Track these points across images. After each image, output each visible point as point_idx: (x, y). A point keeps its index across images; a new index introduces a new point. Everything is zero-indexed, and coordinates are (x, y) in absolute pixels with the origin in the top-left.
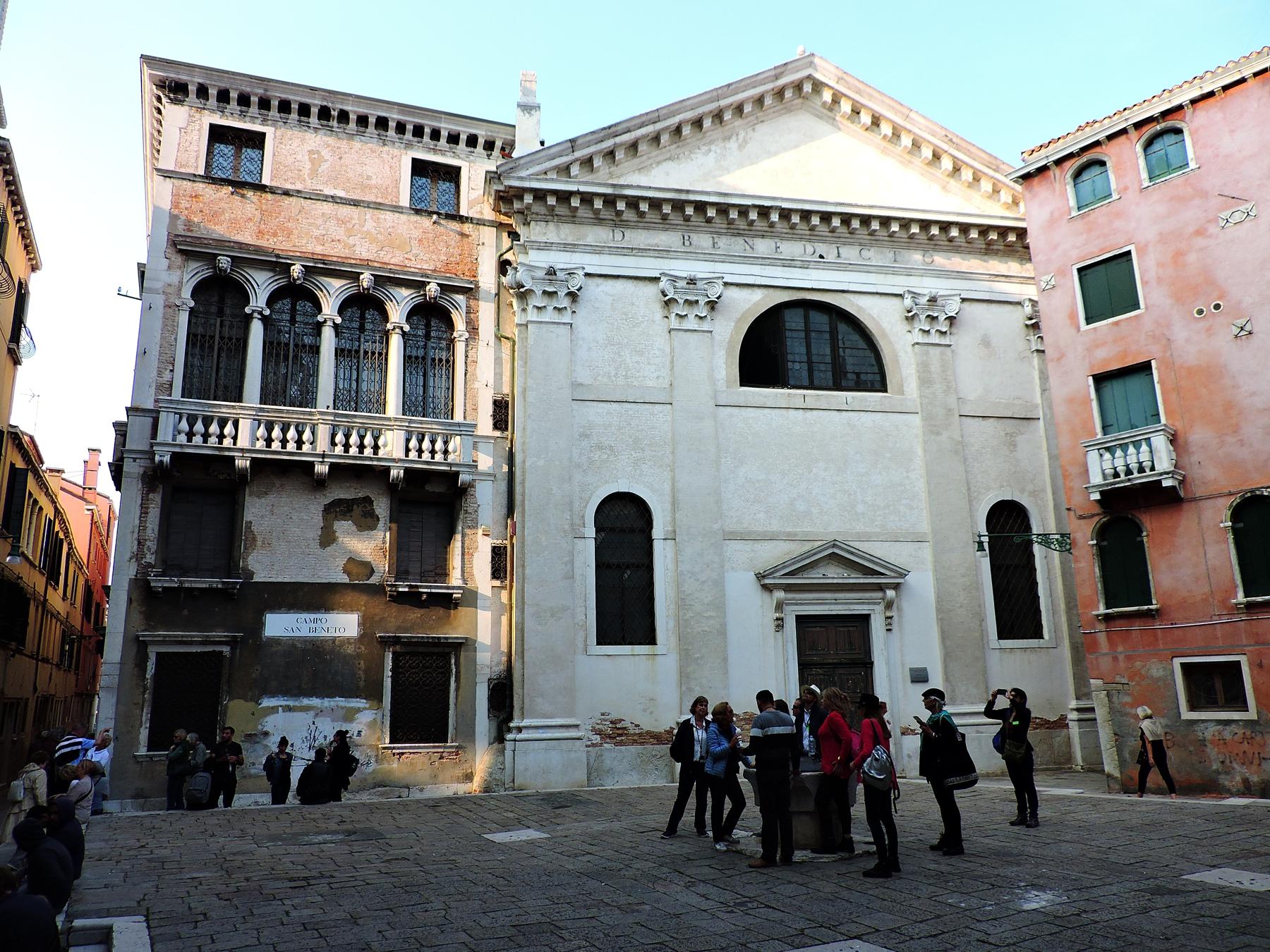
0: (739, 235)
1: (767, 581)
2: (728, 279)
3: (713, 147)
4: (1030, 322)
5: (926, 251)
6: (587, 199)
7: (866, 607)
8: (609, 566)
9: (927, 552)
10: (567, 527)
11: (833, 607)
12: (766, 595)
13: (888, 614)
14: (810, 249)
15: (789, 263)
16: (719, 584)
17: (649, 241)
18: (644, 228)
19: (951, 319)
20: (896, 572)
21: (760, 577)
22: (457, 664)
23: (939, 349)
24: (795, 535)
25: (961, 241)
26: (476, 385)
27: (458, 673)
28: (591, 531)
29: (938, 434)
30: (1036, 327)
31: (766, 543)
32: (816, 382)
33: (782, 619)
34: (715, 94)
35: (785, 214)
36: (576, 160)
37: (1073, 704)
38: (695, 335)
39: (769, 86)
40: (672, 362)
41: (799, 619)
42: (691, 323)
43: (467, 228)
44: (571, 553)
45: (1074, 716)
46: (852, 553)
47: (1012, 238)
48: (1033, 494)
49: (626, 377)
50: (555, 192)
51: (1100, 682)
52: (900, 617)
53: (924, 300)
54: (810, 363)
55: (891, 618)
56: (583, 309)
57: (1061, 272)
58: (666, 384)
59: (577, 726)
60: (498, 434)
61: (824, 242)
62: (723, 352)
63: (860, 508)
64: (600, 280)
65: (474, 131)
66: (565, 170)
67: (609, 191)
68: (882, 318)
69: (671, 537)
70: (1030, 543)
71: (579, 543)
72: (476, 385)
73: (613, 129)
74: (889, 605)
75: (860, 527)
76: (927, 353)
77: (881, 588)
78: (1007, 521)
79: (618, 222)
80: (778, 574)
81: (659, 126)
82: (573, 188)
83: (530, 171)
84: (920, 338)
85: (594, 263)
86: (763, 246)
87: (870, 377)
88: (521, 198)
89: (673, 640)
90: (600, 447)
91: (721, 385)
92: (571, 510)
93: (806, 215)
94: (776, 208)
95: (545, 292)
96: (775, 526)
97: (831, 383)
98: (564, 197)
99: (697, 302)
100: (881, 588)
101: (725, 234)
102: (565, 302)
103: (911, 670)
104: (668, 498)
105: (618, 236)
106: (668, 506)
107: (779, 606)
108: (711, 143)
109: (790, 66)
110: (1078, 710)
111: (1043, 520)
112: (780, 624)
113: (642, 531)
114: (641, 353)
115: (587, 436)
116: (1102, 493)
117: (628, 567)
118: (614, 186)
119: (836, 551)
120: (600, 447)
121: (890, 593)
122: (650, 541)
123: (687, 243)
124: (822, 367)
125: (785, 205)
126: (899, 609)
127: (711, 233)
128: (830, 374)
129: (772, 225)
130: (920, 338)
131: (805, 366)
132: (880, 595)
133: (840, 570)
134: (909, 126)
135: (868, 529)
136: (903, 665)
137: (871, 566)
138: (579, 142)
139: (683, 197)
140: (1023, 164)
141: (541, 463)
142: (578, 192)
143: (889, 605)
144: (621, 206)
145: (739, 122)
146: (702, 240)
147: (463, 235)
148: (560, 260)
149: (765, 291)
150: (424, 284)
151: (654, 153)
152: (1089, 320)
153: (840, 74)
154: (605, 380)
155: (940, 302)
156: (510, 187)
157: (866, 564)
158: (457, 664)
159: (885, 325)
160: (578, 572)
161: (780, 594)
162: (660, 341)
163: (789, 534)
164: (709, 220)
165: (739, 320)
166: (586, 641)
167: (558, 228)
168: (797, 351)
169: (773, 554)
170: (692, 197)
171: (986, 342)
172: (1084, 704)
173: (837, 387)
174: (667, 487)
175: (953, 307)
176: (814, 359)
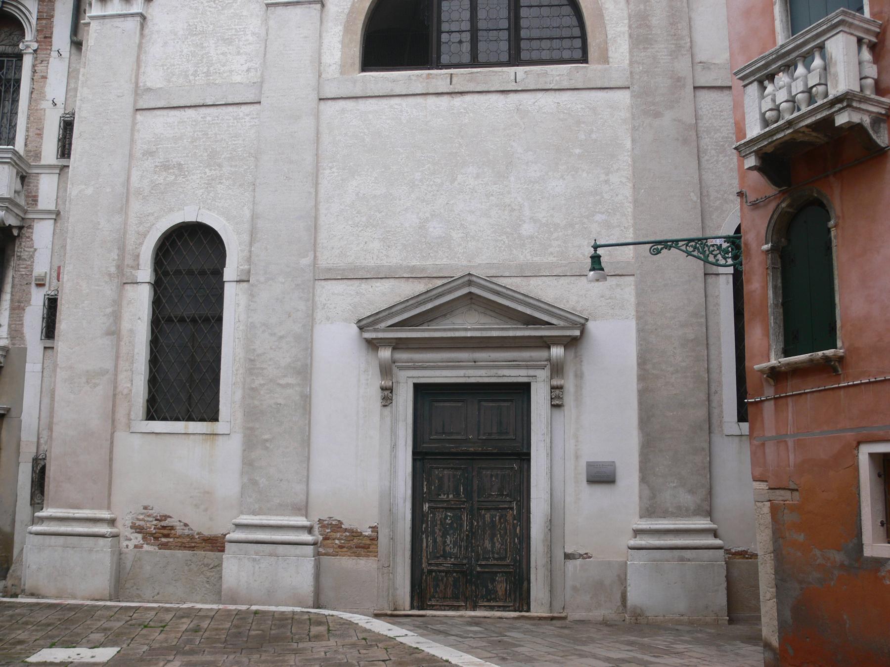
7: (523, 372)
16: (305, 342)
24: (423, 269)
29: (657, 115)
32: (482, 58)
33: (391, 390)
41: (420, 390)
46: (498, 293)
49: (208, 74)
52: (579, 388)
54: (474, 31)
63: (527, 229)
75: (524, 256)
77: (545, 343)
80: (383, 325)
90: (165, 167)
96: (395, 258)
106: (246, 237)
107: (386, 370)
112: (387, 395)
114: (229, 41)
119: (474, 290)
120: (165, 167)
126: (579, 376)
131: (466, 37)
133: (484, 319)
137: (528, 311)
141: (90, 191)
154: (181, 81)
157: (520, 308)
162: (254, 24)
163: (413, 269)
168: (455, 16)
169: (382, 295)
176: (481, 25)
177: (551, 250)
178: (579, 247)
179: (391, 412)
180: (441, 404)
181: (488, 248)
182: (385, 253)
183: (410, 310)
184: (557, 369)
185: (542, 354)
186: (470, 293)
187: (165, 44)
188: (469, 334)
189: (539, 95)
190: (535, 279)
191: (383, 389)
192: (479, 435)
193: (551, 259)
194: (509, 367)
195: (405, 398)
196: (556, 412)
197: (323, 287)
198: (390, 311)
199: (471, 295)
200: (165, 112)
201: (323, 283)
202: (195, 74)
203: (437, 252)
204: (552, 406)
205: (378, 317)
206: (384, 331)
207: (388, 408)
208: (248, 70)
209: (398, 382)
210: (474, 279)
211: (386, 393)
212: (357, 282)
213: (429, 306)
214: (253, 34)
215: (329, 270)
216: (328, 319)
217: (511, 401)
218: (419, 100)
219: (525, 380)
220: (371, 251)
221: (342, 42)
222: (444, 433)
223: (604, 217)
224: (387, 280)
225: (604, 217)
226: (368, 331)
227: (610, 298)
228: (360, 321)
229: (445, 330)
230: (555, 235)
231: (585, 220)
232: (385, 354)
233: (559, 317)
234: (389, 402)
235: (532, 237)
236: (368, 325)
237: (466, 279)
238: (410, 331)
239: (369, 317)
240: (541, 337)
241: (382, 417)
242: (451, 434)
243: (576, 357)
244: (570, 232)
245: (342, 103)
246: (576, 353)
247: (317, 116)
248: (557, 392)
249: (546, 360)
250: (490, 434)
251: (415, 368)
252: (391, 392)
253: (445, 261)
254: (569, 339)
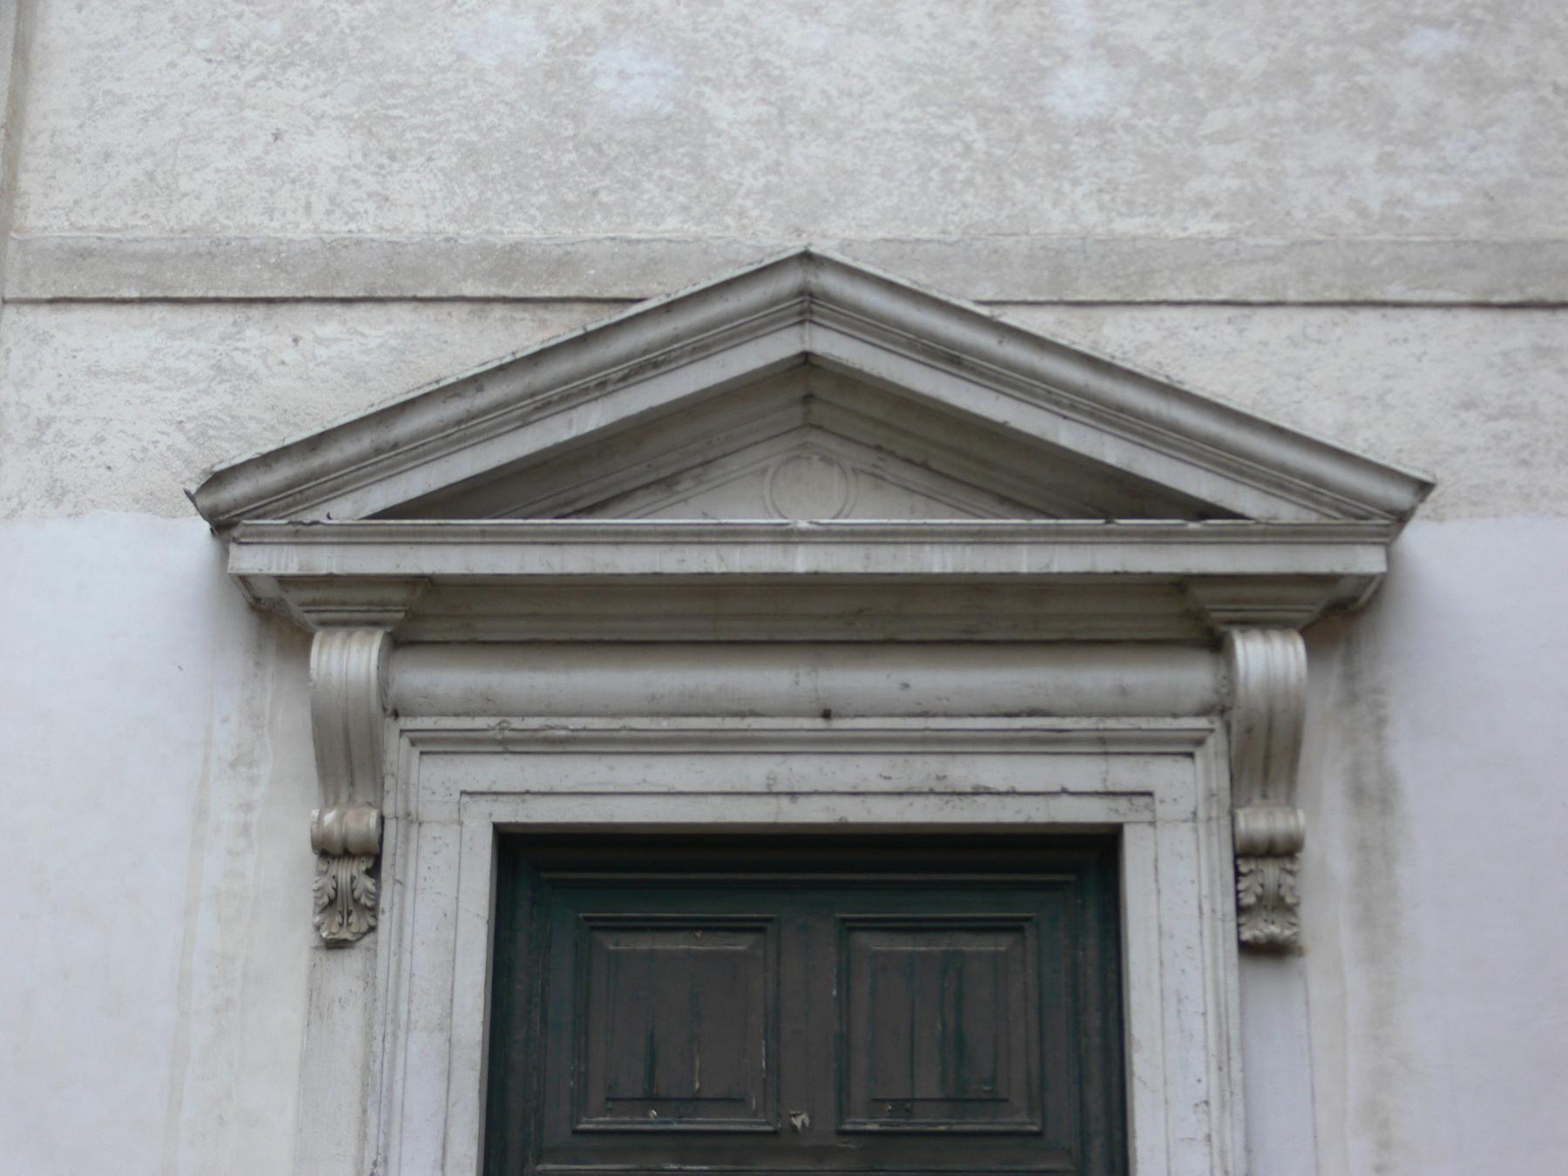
7: (1082, 772)
24: (566, 263)
33: (372, 856)
46: (951, 358)
52: (1375, 857)
55: (1285, 851)
63: (1079, 89)
75: (1071, 210)
77: (1196, 618)
80: (343, 510)
96: (419, 209)
100: (1196, 618)
107: (348, 751)
112: (351, 886)
121: (1267, 658)
126: (1374, 796)
133: (873, 510)
137: (1112, 451)
161: (348, 659)
163: (511, 257)
177: (1198, 185)
178: (1340, 173)
179: (369, 981)
180: (643, 943)
181: (886, 173)
182: (371, 183)
183: (490, 435)
184: (1264, 752)
185: (1191, 677)
186: (806, 360)
188: (802, 561)
190: (1125, 315)
192: (842, 1111)
193: (1199, 226)
194: (1007, 744)
195: (445, 907)
196: (1265, 974)
197: (43, 339)
198: (382, 436)
199: (816, 371)
201: (44, 318)
203: (635, 186)
204: (1249, 949)
205: (316, 462)
206: (348, 535)
207: (352, 961)
209: (411, 819)
210: (830, 282)
211: (345, 872)
212: (221, 319)
213: (592, 418)
215: (80, 255)
216: (56, 493)
217: (1013, 927)
219: (1093, 813)
220: (308, 178)
222: (652, 1099)
223: (1452, 41)
224: (377, 311)
225: (1452, 41)
226: (260, 539)
227: (1507, 412)
228: (217, 479)
229: (672, 537)
230: (1217, 120)
231: (1361, 56)
232: (348, 659)
233: (1276, 480)
234: (358, 923)
235: (1101, 126)
236: (260, 506)
237: (789, 281)
238: (486, 538)
239: (266, 460)
240: (1181, 584)
241: (317, 1005)
242: (696, 1101)
243: (1352, 698)
244: (1288, 106)
246: (1350, 677)
248: (1271, 872)
249: (1204, 712)
250: (904, 1106)
251: (506, 745)
252: (374, 872)
253: (672, 225)
254: (1321, 597)
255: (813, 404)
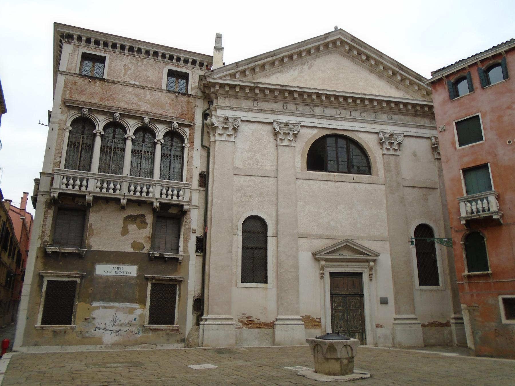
0: (308, 105)
1: (317, 257)
2: (303, 124)
3: (297, 68)
4: (433, 146)
5: (389, 114)
6: (242, 88)
7: (361, 269)
8: (248, 248)
9: (387, 246)
10: (230, 230)
11: (346, 269)
12: (317, 263)
13: (371, 273)
14: (338, 112)
15: (329, 118)
16: (296, 257)
17: (268, 107)
18: (267, 101)
19: (399, 144)
20: (374, 254)
21: (314, 254)
22: (180, 290)
23: (393, 157)
24: (330, 236)
25: (404, 110)
26: (192, 167)
27: (180, 294)
28: (240, 232)
29: (394, 194)
30: (437, 148)
31: (317, 240)
32: (340, 170)
34: (298, 45)
35: (328, 96)
36: (238, 72)
37: (453, 316)
38: (288, 148)
39: (322, 42)
40: (277, 159)
41: (332, 274)
42: (286, 143)
43: (191, 99)
44: (231, 242)
45: (453, 321)
46: (355, 245)
47: (426, 109)
48: (435, 221)
49: (257, 165)
50: (229, 85)
51: (465, 305)
53: (387, 135)
55: (372, 274)
56: (240, 135)
57: (449, 124)
58: (274, 168)
59: (231, 319)
60: (201, 188)
61: (345, 109)
62: (300, 156)
63: (359, 225)
64: (247, 123)
65: (195, 58)
66: (233, 76)
67: (252, 85)
68: (369, 142)
69: (276, 236)
70: (433, 243)
71: (235, 238)
72: (192, 167)
73: (254, 59)
74: (371, 269)
76: (389, 158)
77: (367, 261)
78: (423, 232)
79: (255, 99)
81: (274, 58)
82: (237, 83)
83: (218, 76)
84: (385, 152)
85: (244, 115)
86: (318, 110)
87: (364, 168)
88: (214, 87)
89: (275, 282)
90: (245, 195)
91: (298, 170)
92: (232, 223)
93: (337, 97)
94: (324, 94)
95: (223, 128)
96: (321, 232)
97: (346, 170)
98: (232, 87)
99: (289, 133)
100: (367, 261)
101: (302, 105)
102: (231, 132)
103: (381, 298)
104: (274, 219)
105: (256, 104)
106: (274, 222)
107: (322, 268)
108: (296, 66)
109: (331, 34)
110: (456, 319)
111: (439, 233)
112: (322, 276)
113: (262, 233)
114: (264, 155)
115: (240, 190)
116: (466, 221)
117: (256, 248)
118: (254, 83)
120: (245, 195)
121: (372, 263)
122: (266, 237)
123: (285, 108)
124: (343, 163)
125: (328, 93)
126: (376, 271)
127: (296, 104)
128: (346, 166)
129: (322, 101)
130: (385, 152)
132: (367, 264)
133: (349, 253)
134: (382, 61)
135: (362, 235)
136: (377, 296)
138: (240, 64)
139: (284, 88)
140: (432, 77)
141: (219, 202)
142: (239, 85)
143: (371, 269)
144: (257, 91)
145: (308, 57)
146: (292, 107)
147: (189, 102)
148: (230, 114)
149: (319, 130)
150: (171, 123)
151: (272, 70)
152: (460, 145)
153: (352, 38)
154: (248, 166)
155: (395, 136)
156: (210, 82)
158: (180, 290)
159: (371, 146)
160: (234, 249)
161: (323, 263)
163: (327, 236)
164: (295, 99)
165: (306, 142)
166: (236, 281)
167: (230, 100)
169: (319, 244)
170: (288, 88)
171: (415, 154)
172: (457, 316)
173: (349, 172)
174: (274, 214)
175: (400, 139)
187: (242, 153)
188: (347, 257)
189: (360, 184)
191: (321, 274)
198: (325, 249)
200: (243, 176)
202: (253, 164)
208: (271, 166)
213: (335, 248)
214: (272, 154)
215: (302, 235)
216: (302, 250)
218: (326, 182)
221: (301, 160)
245: (302, 181)
247: (295, 184)
251: (330, 267)
255: (347, 247)
